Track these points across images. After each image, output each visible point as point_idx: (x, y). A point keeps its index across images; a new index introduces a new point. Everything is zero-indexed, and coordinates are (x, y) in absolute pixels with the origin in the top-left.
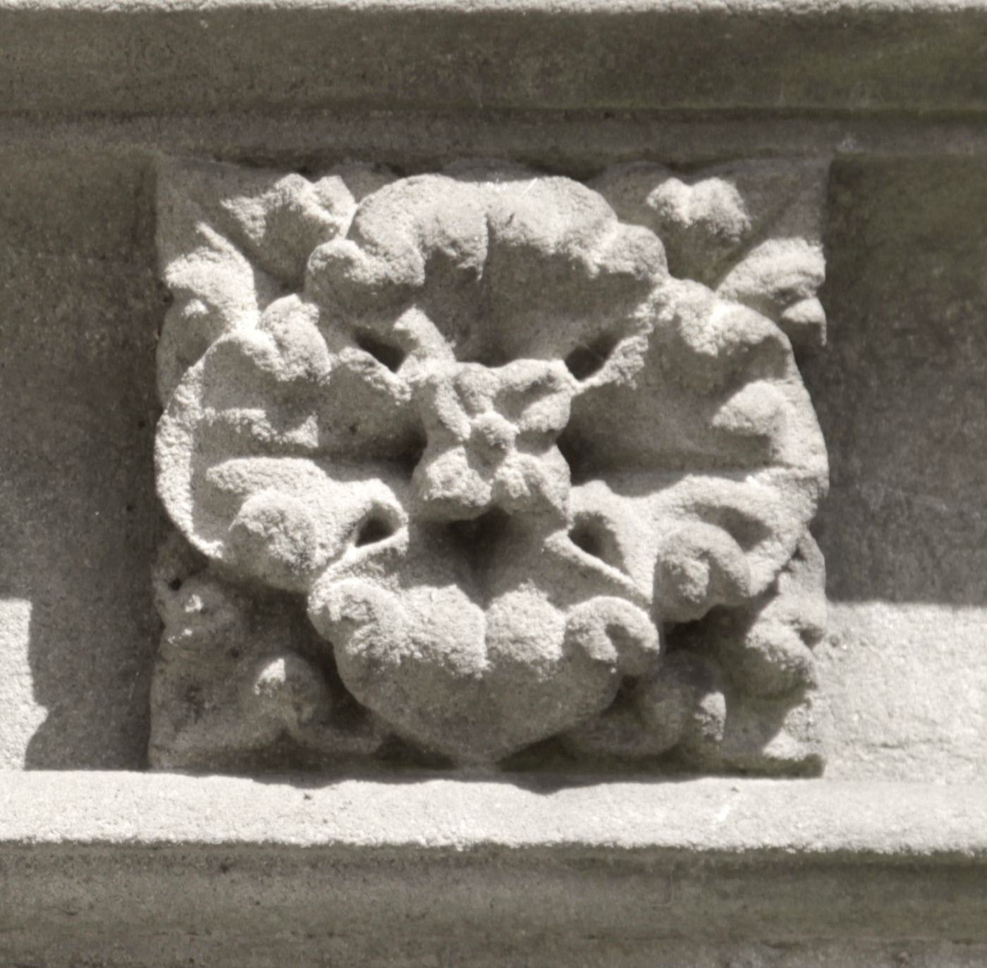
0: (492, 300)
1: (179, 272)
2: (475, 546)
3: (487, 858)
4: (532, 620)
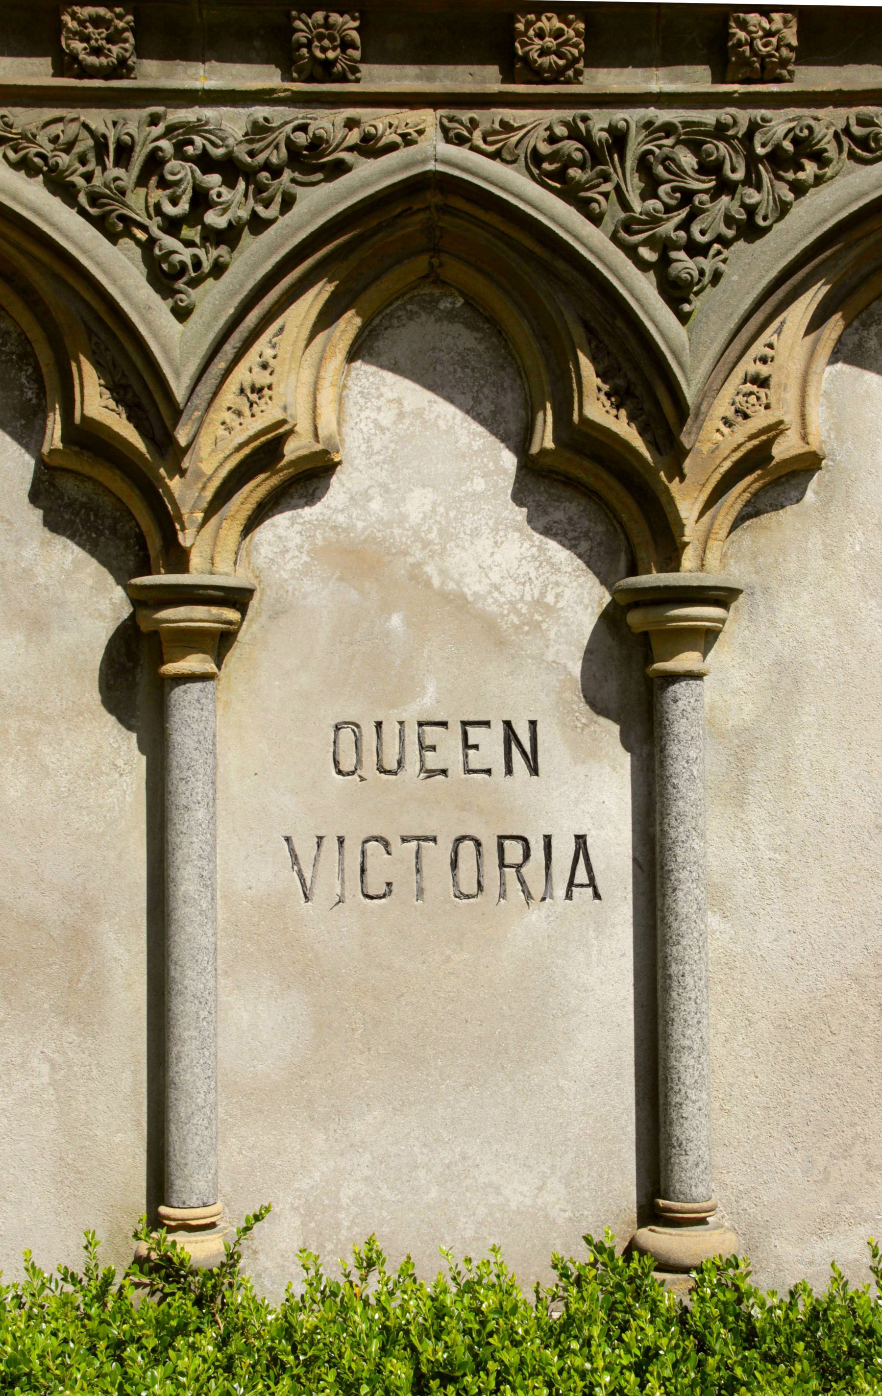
0: (97, 21)
1: (63, 18)
2: (97, 51)
3: (99, 88)
4: (104, 61)
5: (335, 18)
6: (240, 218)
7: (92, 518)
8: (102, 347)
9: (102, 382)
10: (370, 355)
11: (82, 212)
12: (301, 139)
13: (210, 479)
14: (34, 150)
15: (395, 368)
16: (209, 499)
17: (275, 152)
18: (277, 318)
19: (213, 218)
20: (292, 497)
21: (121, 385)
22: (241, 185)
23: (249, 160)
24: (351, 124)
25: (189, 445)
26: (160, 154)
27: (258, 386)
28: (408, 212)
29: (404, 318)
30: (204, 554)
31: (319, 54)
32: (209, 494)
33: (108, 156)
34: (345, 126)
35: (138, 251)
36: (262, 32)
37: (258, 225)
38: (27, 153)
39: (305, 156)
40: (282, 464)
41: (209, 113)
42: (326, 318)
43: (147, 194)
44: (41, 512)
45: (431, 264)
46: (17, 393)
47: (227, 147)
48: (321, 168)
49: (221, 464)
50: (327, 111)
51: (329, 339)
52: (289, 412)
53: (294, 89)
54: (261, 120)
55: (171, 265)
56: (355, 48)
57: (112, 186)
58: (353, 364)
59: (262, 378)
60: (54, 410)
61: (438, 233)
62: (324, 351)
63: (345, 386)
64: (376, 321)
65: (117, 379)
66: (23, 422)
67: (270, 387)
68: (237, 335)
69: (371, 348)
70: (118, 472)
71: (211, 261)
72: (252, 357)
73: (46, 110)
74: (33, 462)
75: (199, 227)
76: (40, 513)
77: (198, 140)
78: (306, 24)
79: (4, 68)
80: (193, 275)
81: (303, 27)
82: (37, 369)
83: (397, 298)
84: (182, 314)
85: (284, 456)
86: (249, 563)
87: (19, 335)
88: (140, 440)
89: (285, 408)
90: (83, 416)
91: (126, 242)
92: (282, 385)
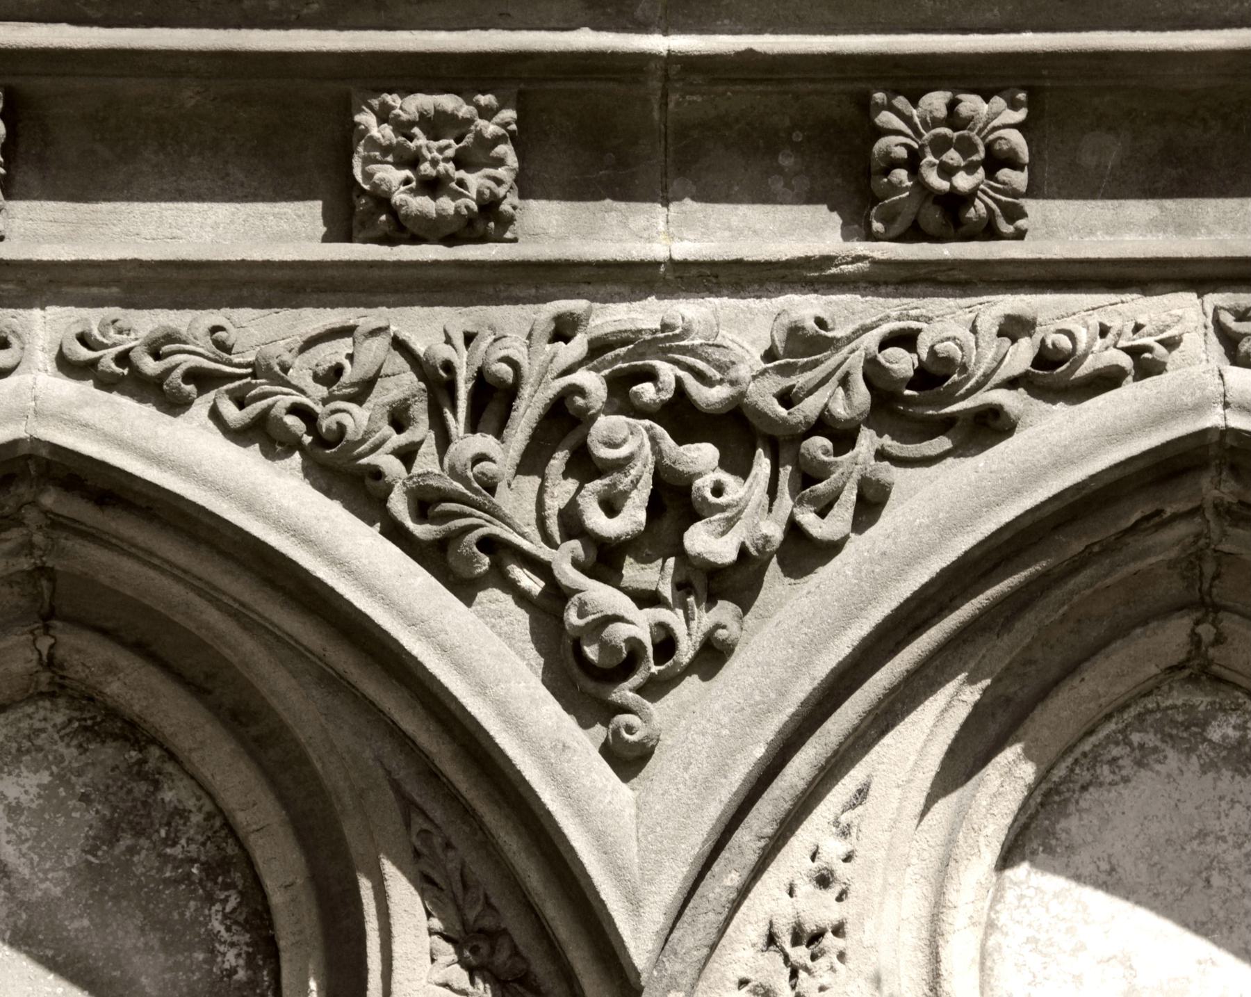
0: (436, 124)
1: (357, 118)
2: (432, 186)
3: (436, 263)
4: (447, 205)
5: (971, 104)
6: (767, 539)
8: (437, 841)
9: (437, 924)
10: (1049, 850)
11: (395, 532)
12: (902, 362)
14: (284, 400)
15: (1110, 880)
17: (840, 391)
19: (703, 541)
21: (481, 931)
22: (762, 465)
23: (783, 412)
24: (1014, 328)
26: (579, 401)
27: (810, 927)
28: (1156, 521)
31: (935, 180)
33: (455, 413)
34: (1000, 334)
35: (521, 619)
36: (798, 137)
37: (803, 553)
38: (271, 407)
39: (909, 401)
41: (691, 311)
42: (963, 762)
43: (542, 490)
45: (1195, 640)
46: (200, 956)
47: (733, 383)
48: (945, 425)
50: (951, 302)
51: (961, 814)
53: (878, 255)
54: (810, 325)
55: (607, 648)
56: (1015, 165)
57: (470, 474)
58: (1009, 873)
59: (819, 909)
61: (1209, 568)
62: (951, 842)
63: (991, 926)
64: (1060, 772)
65: (471, 915)
67: (839, 930)
69: (1050, 833)
71: (698, 636)
73: (307, 312)
75: (671, 561)
77: (667, 372)
78: (908, 120)
79: (215, 226)
80: (655, 669)
81: (898, 124)
82: (255, 892)
83: (1108, 717)
84: (627, 759)
87: (209, 817)
91: (493, 598)
92: (869, 925)
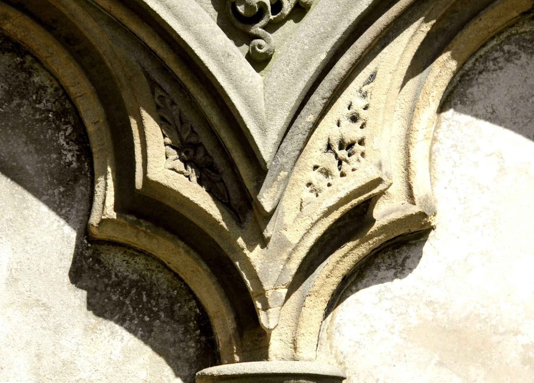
7: (145, 299)
8: (168, 101)
9: (168, 140)
10: (463, 103)
13: (295, 249)
15: (492, 117)
16: (294, 272)
18: (368, 63)
20: (378, 268)
21: (190, 144)
25: (274, 210)
27: (347, 141)
29: (501, 60)
30: (284, 337)
32: (294, 266)
40: (372, 229)
42: (421, 62)
44: (84, 293)
46: (54, 156)
49: (308, 232)
52: (384, 170)
58: (443, 114)
59: (352, 132)
60: (105, 174)
63: (434, 139)
64: (469, 65)
65: (185, 136)
66: (62, 189)
67: (361, 142)
68: (327, 83)
69: (464, 95)
70: (181, 243)
72: (340, 109)
74: (74, 235)
76: (83, 294)
80: (272, 17)
83: (493, 38)
84: (259, 61)
85: (374, 221)
86: (331, 347)
87: (56, 90)
88: (214, 206)
89: (380, 166)
90: (146, 180)
92: (376, 139)
